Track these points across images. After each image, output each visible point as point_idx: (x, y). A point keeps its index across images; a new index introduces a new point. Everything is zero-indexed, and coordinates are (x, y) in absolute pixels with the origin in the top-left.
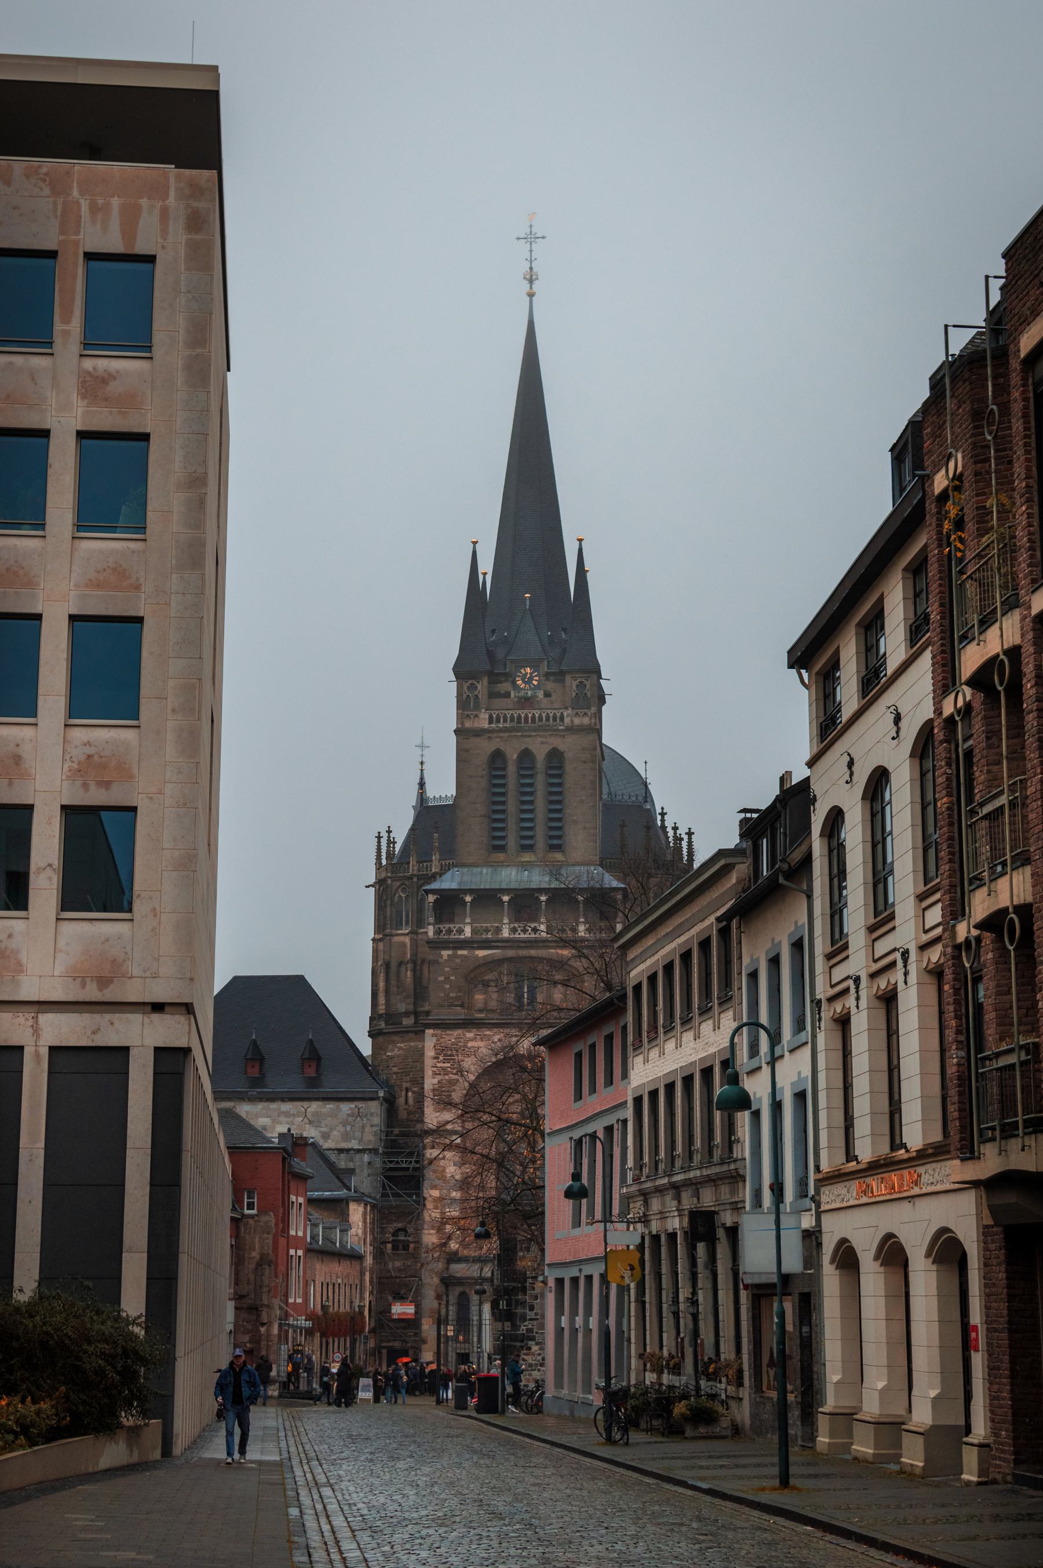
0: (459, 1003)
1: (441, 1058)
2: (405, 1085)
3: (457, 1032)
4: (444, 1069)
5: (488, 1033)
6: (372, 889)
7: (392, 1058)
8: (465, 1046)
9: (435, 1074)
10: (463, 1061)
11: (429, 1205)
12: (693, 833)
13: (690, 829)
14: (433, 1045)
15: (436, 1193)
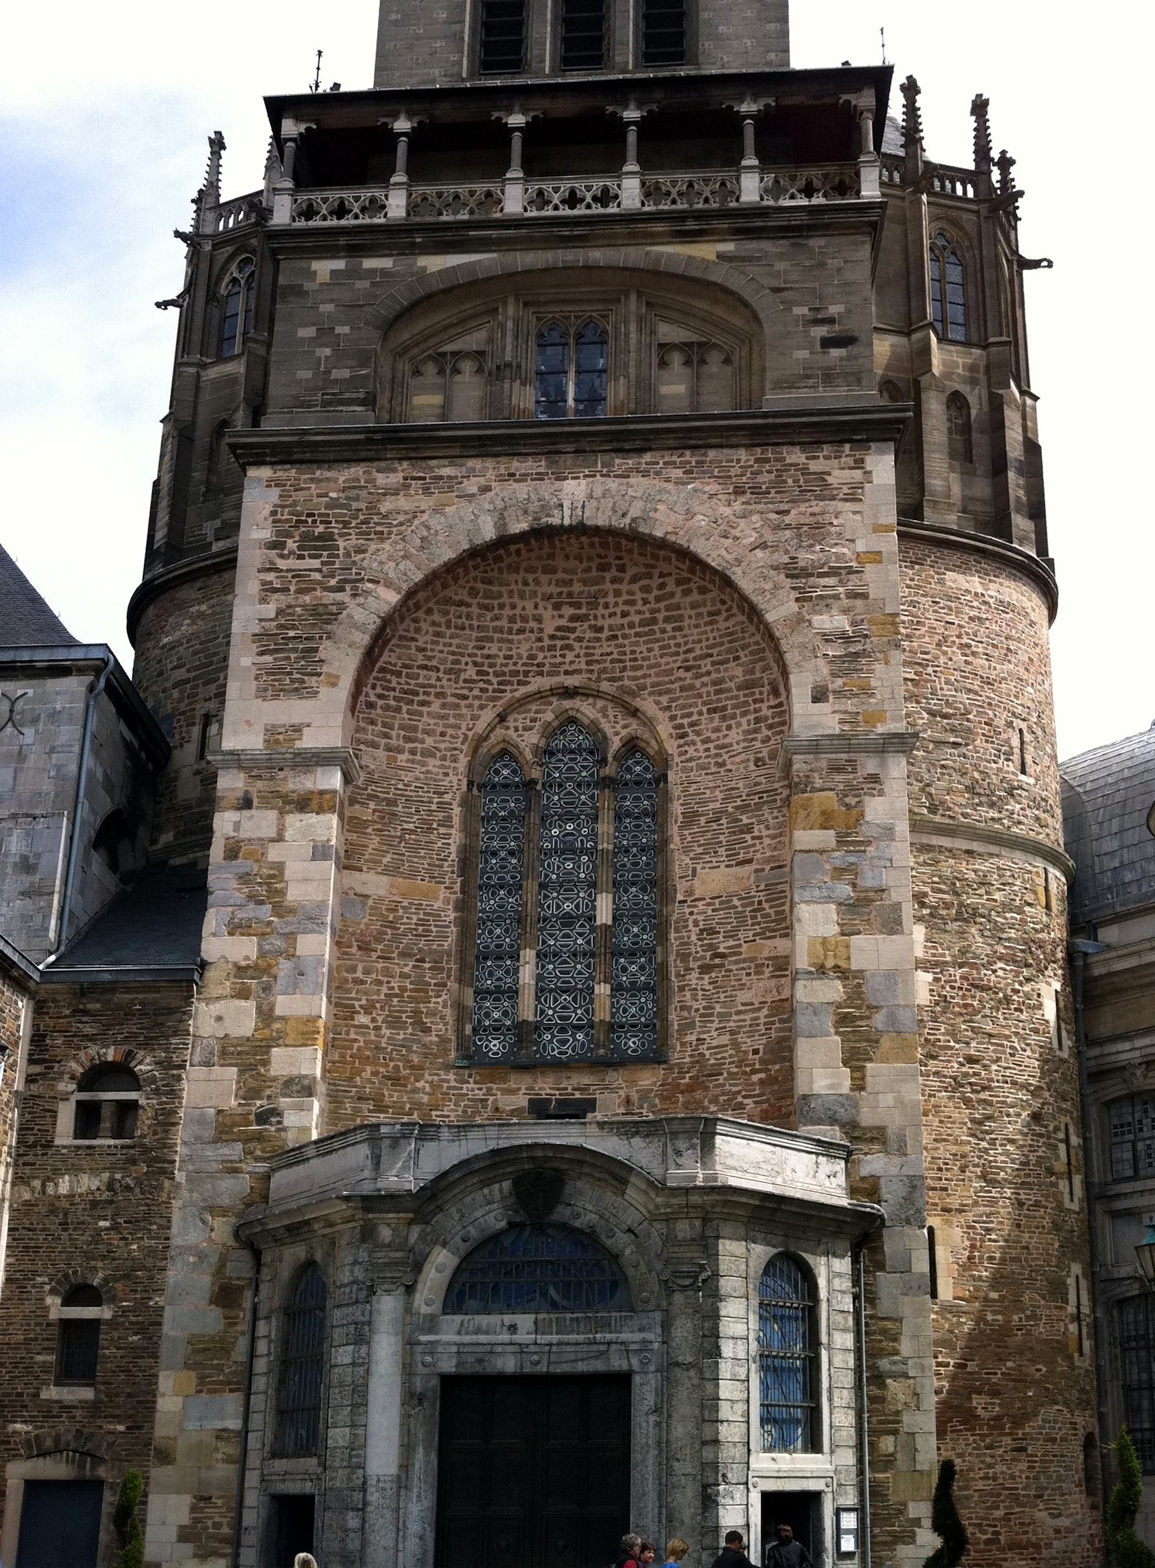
0: (362, 396)
1: (291, 544)
2: (201, 708)
3: (344, 475)
4: (298, 575)
5: (446, 471)
6: (174, 312)
7: (172, 647)
8: (372, 508)
9: (268, 590)
10: (361, 551)
11: (217, 981)
12: (1012, 162)
13: (1003, 152)
14: (268, 508)
15: (245, 949)
